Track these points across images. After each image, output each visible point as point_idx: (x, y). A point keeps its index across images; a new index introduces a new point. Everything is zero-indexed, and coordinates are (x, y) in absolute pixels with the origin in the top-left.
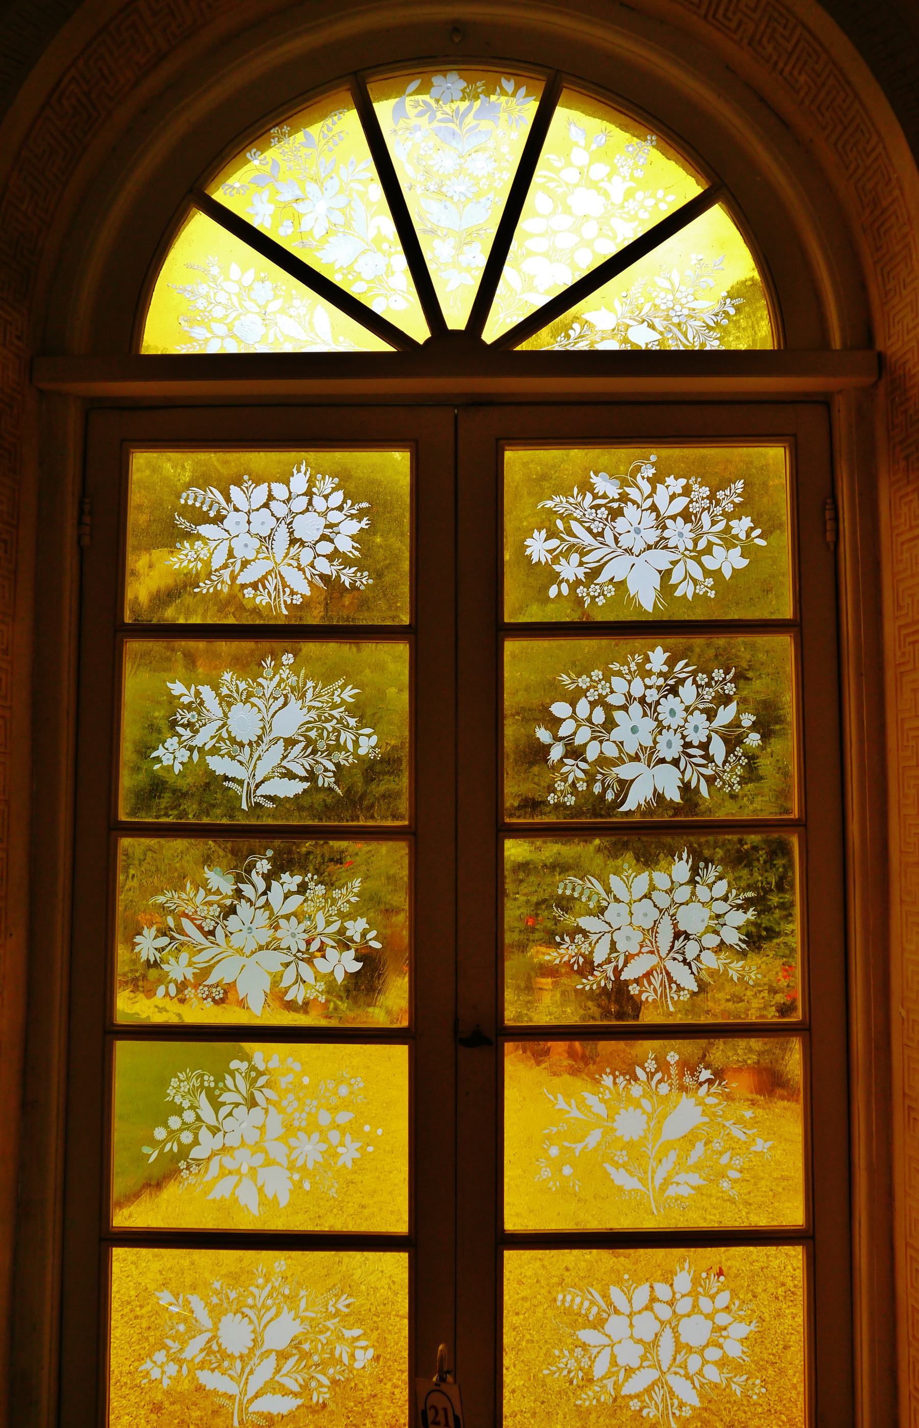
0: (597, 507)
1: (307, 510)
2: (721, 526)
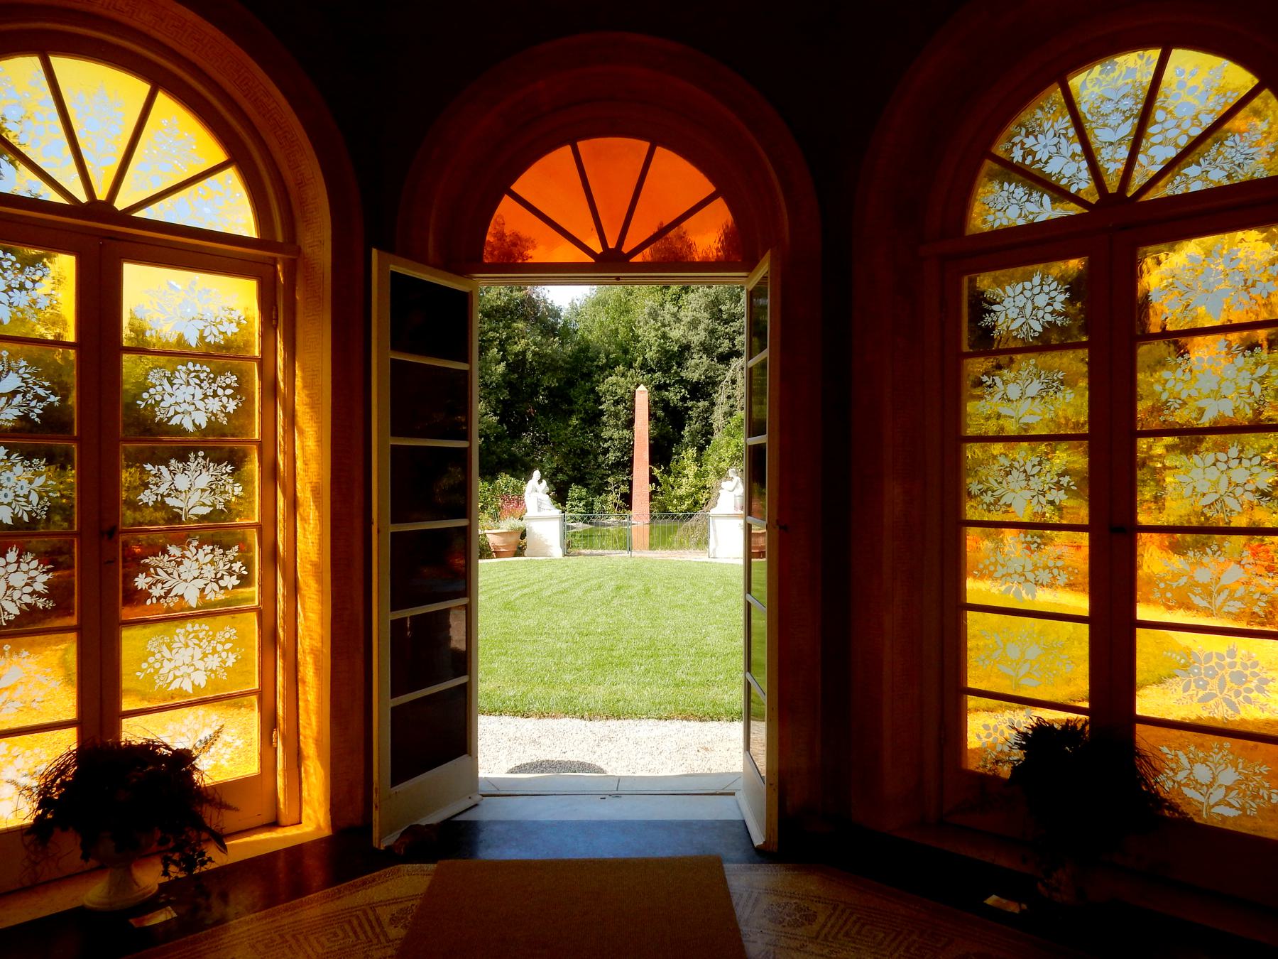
0: (170, 561)
1: (17, 571)
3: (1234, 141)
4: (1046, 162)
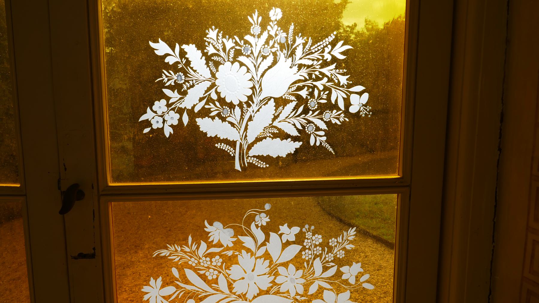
0: (211, 255)
2: (332, 272)
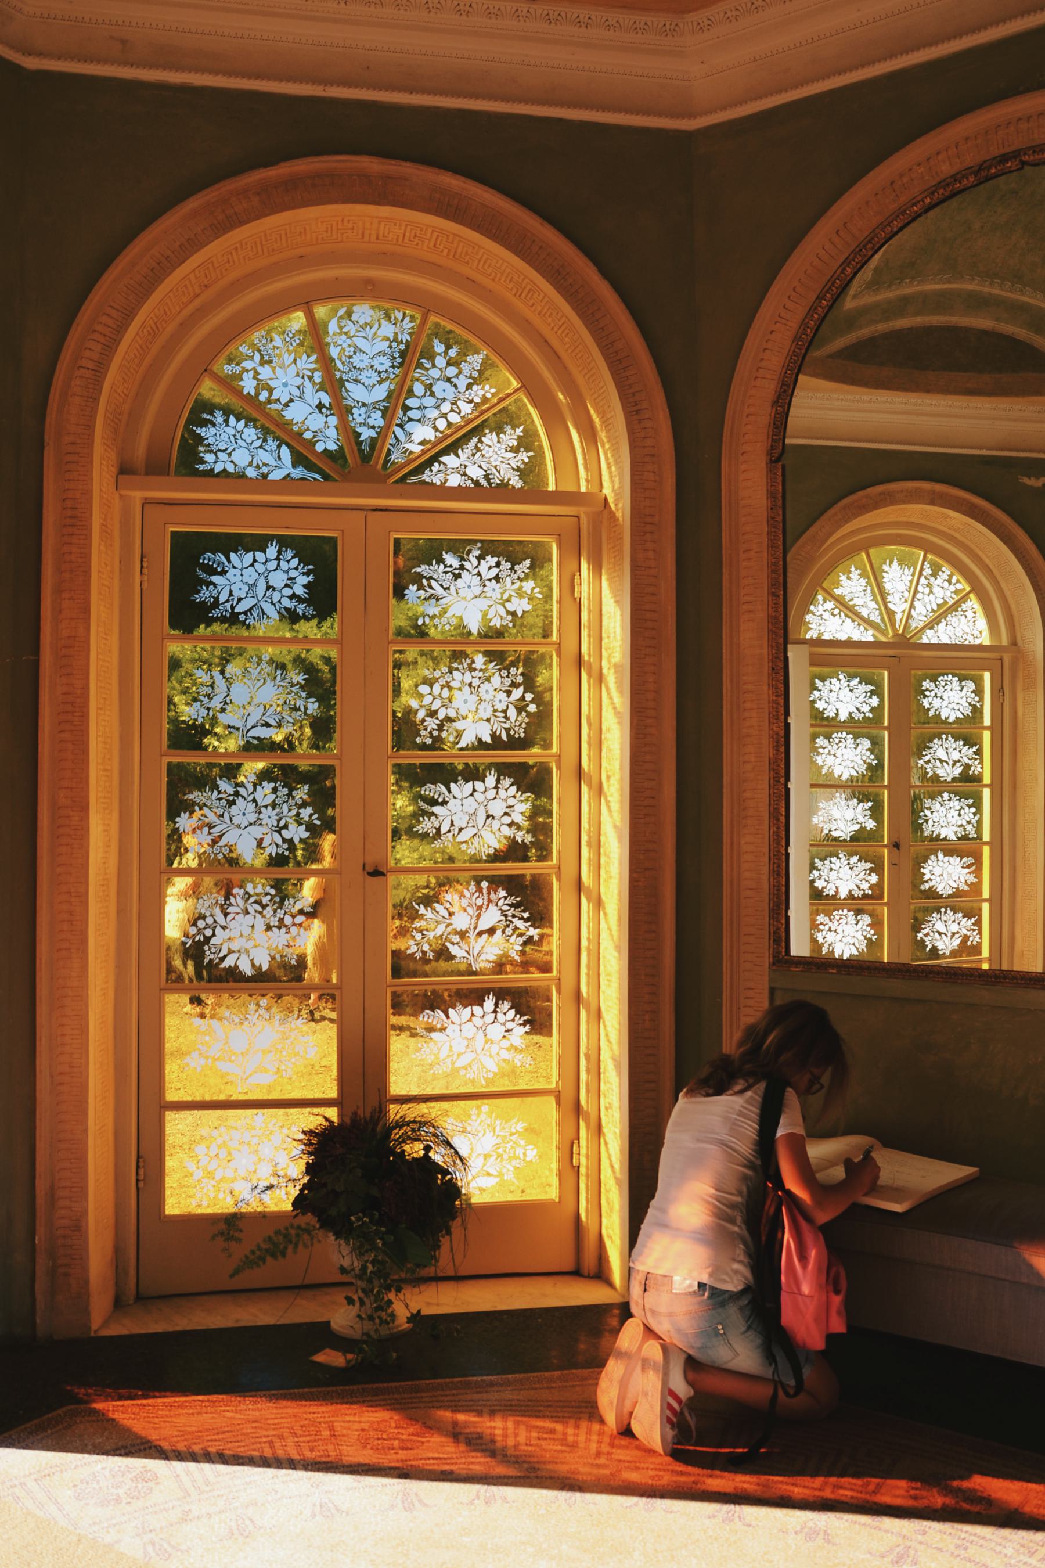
3: (492, 440)
4: (286, 405)
